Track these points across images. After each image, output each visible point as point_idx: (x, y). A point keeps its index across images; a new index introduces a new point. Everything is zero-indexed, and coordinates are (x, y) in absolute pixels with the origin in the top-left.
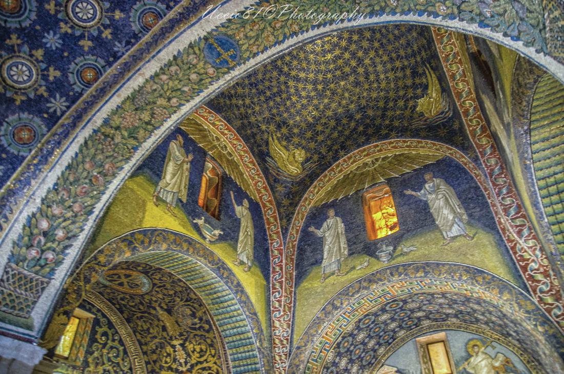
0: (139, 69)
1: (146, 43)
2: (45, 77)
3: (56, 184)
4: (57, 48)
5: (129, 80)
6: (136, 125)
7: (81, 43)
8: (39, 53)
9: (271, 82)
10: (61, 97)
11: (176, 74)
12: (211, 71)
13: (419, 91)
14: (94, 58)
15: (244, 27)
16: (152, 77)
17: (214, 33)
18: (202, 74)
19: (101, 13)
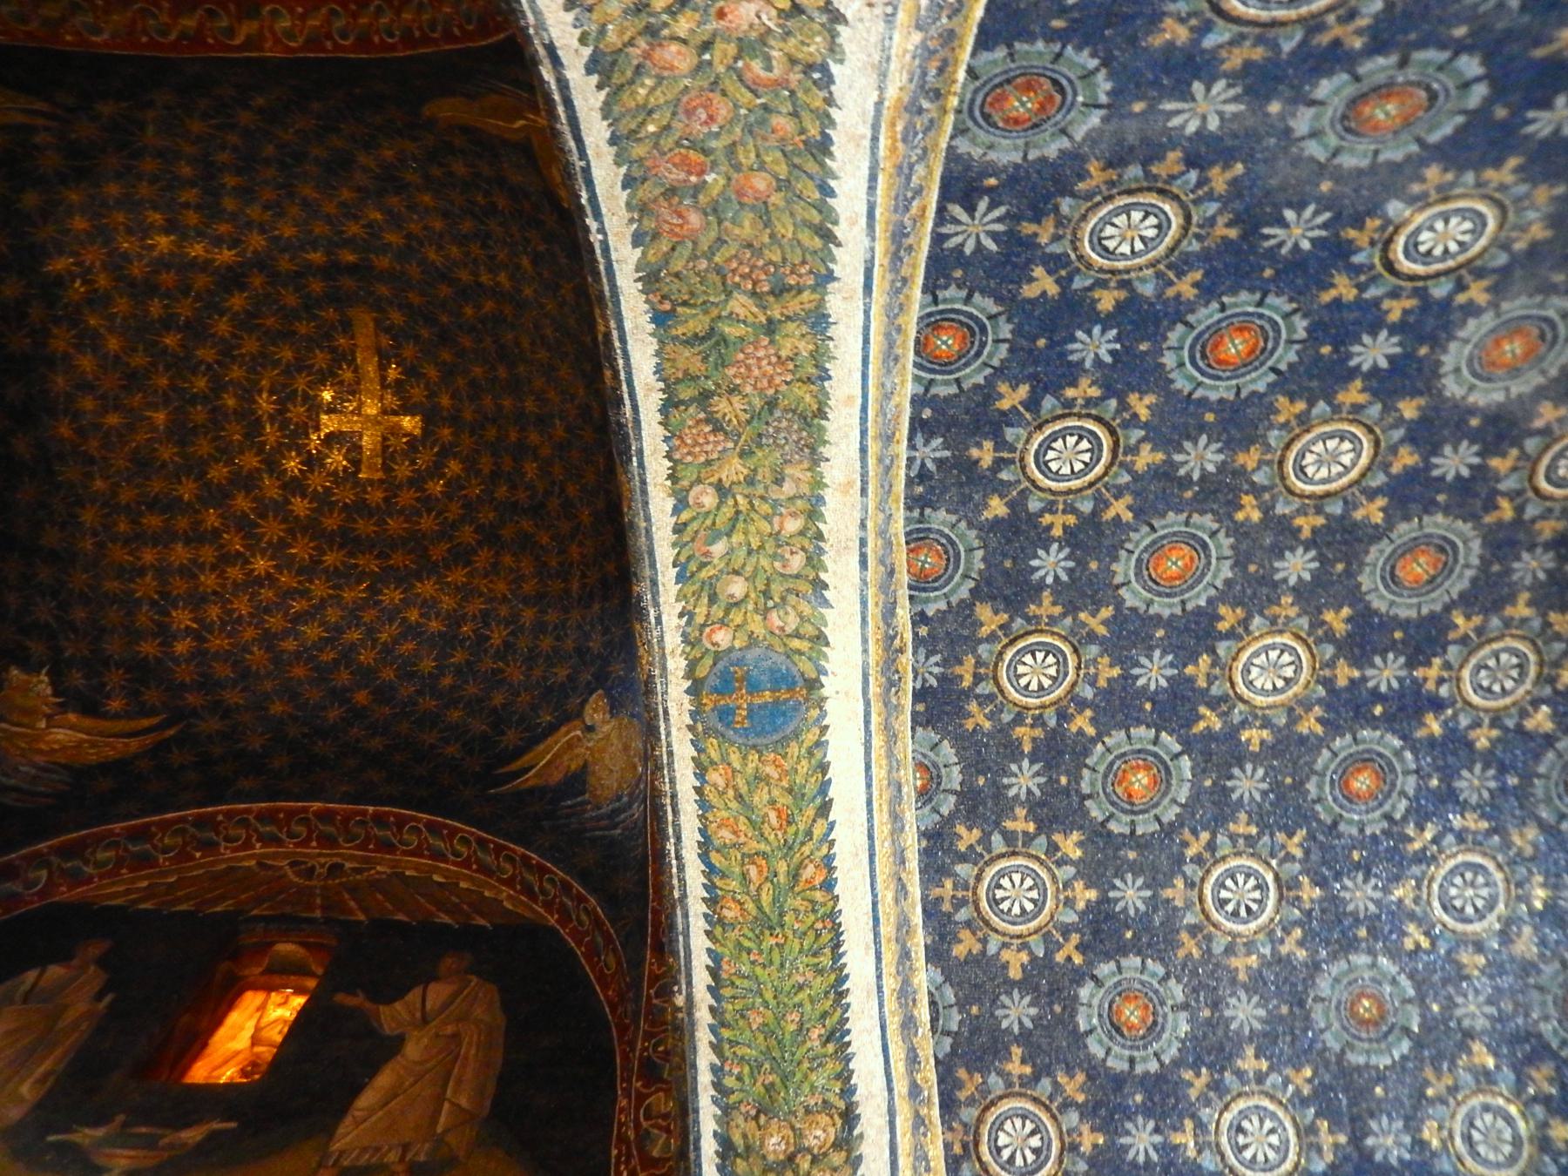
0: (864, 491)
4: (1074, 339)
5: (863, 450)
6: (731, 372)
8: (1107, 301)
9: (266, 208)
11: (774, 557)
12: (723, 638)
13: (77, 679)
15: (790, 791)
16: (820, 500)
18: (727, 612)
19: (1033, 482)
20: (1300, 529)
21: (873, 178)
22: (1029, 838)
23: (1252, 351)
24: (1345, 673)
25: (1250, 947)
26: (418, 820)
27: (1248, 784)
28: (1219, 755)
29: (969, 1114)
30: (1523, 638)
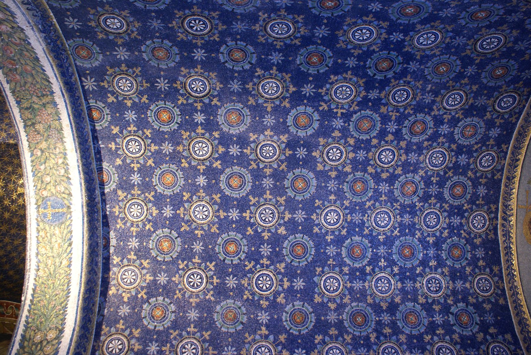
1: (91, 163)
2: (113, 93)
3: (29, 44)
7: (118, 128)
8: (129, 103)
10: (93, 89)
11: (57, 170)
12: (45, 193)
14: (104, 126)
16: (65, 154)
17: (69, 216)
20: (200, 170)
21: (52, 67)
22: (135, 261)
23: (169, 118)
24: (222, 214)
25: (197, 296)
26: (13, 304)
27: (198, 247)
28: (189, 237)
29: (102, 338)
30: (271, 205)
